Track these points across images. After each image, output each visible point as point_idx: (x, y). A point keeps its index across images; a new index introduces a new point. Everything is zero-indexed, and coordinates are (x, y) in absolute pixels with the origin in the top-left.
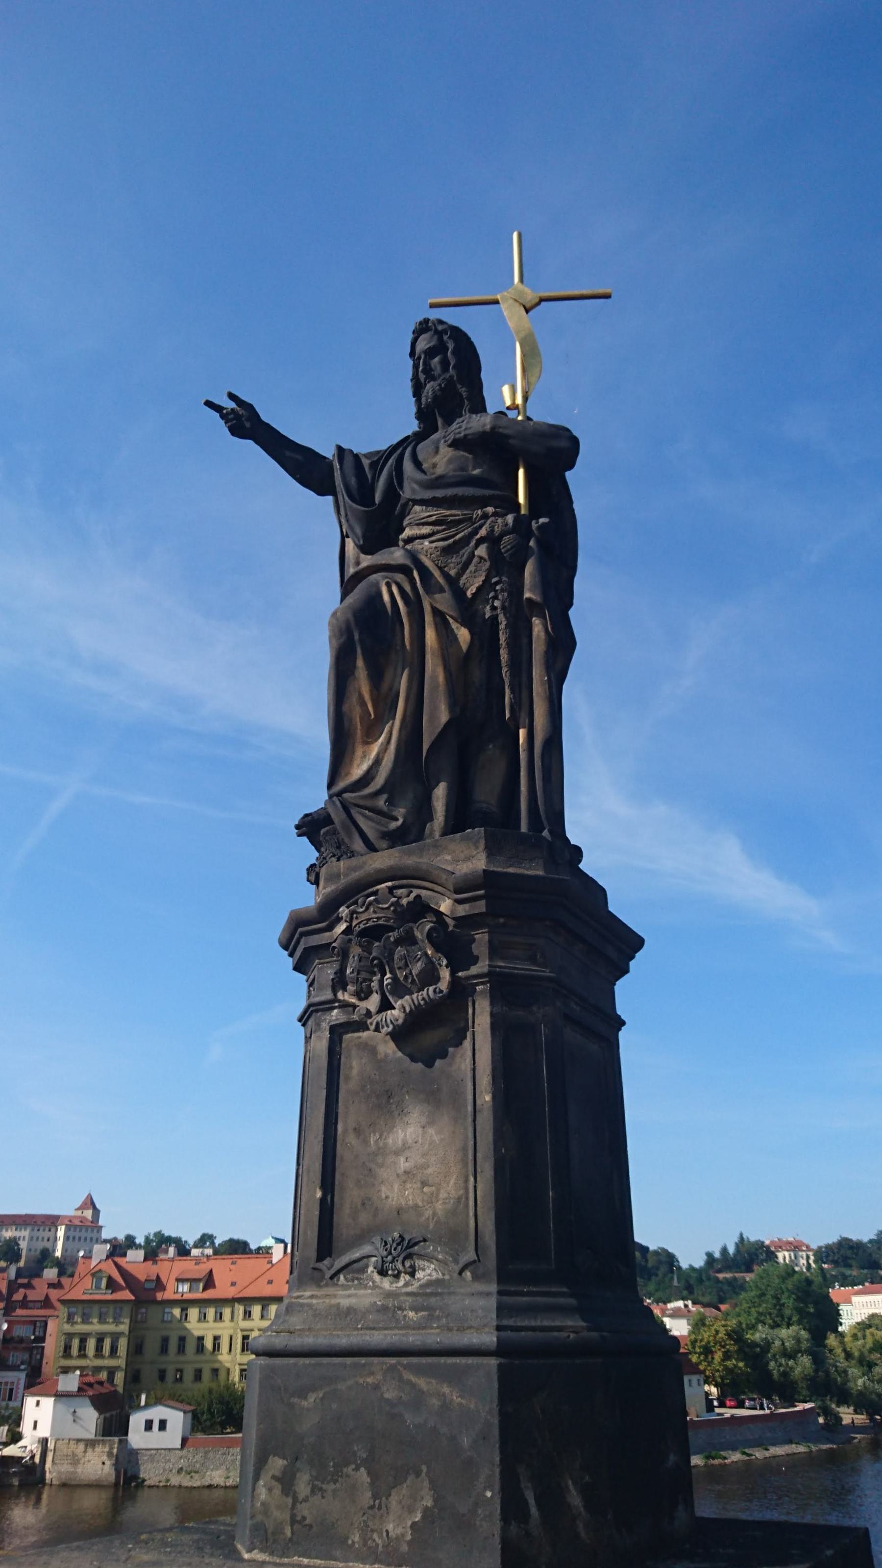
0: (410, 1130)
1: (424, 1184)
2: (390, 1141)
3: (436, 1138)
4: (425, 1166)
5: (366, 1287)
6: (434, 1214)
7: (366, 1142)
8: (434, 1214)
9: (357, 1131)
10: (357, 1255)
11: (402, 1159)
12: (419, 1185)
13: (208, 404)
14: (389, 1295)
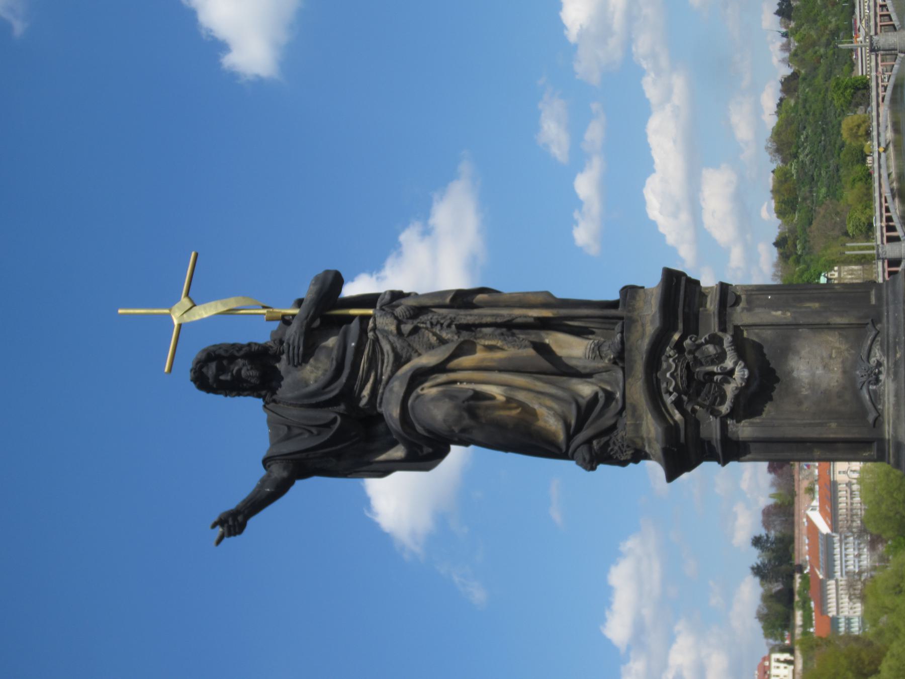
0: (802, 367)
1: (830, 357)
2: (807, 381)
3: (807, 349)
4: (822, 358)
5: (884, 391)
6: (847, 350)
7: (806, 397)
8: (847, 350)
9: (800, 403)
10: (867, 397)
11: (818, 372)
12: (832, 361)
13: (219, 542)
14: (888, 374)
